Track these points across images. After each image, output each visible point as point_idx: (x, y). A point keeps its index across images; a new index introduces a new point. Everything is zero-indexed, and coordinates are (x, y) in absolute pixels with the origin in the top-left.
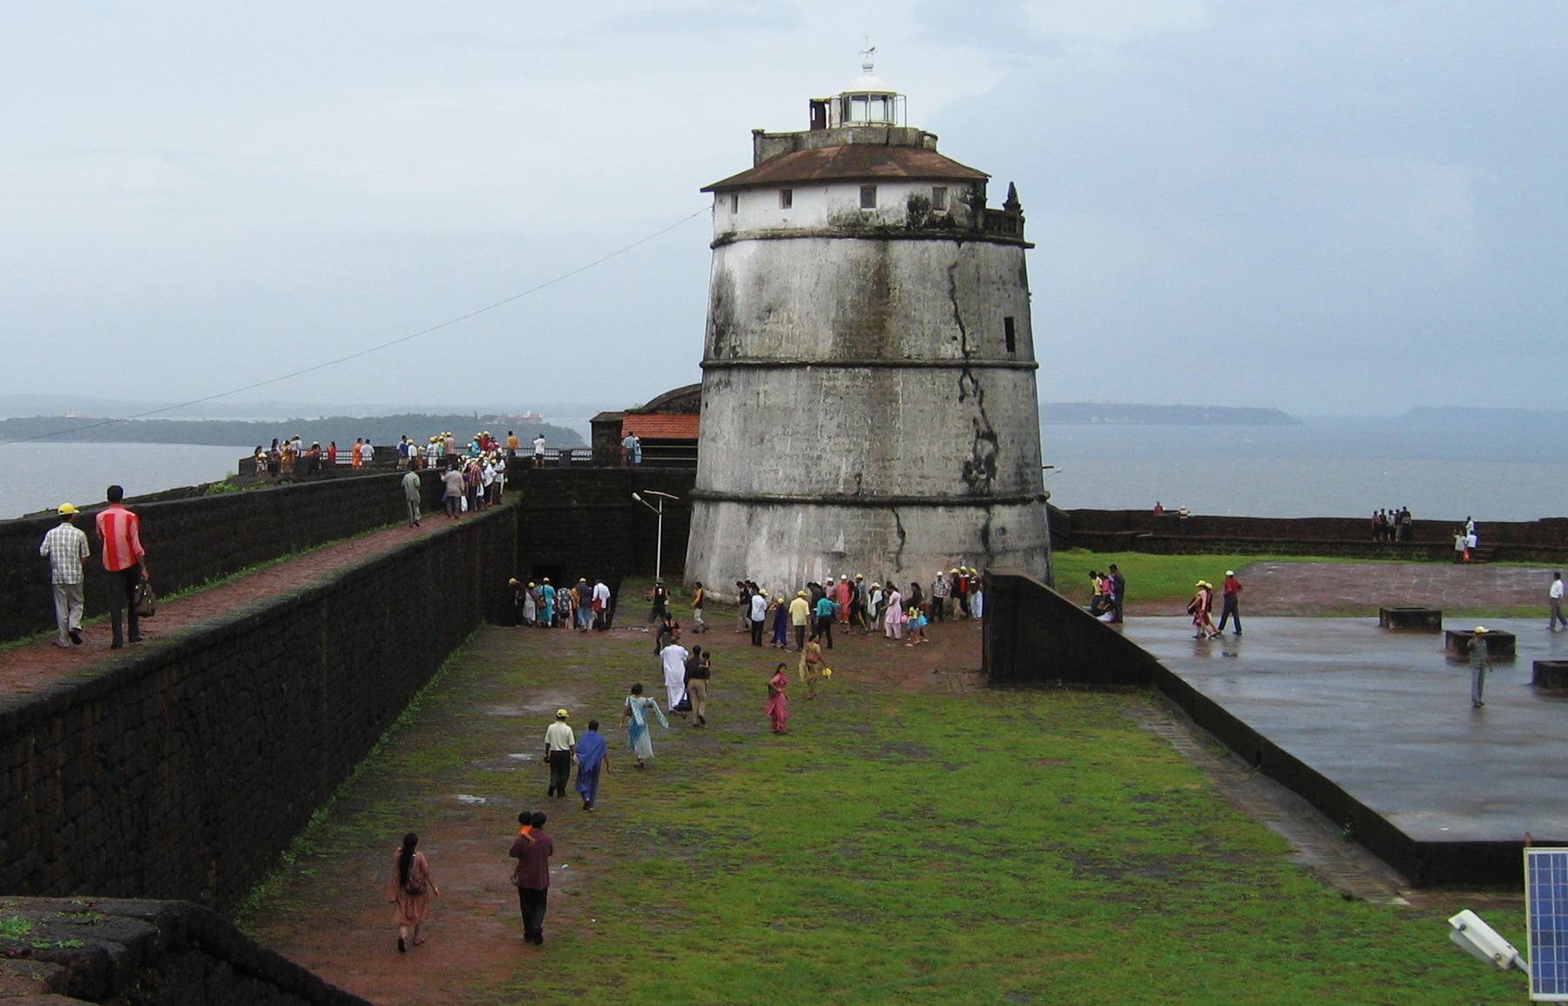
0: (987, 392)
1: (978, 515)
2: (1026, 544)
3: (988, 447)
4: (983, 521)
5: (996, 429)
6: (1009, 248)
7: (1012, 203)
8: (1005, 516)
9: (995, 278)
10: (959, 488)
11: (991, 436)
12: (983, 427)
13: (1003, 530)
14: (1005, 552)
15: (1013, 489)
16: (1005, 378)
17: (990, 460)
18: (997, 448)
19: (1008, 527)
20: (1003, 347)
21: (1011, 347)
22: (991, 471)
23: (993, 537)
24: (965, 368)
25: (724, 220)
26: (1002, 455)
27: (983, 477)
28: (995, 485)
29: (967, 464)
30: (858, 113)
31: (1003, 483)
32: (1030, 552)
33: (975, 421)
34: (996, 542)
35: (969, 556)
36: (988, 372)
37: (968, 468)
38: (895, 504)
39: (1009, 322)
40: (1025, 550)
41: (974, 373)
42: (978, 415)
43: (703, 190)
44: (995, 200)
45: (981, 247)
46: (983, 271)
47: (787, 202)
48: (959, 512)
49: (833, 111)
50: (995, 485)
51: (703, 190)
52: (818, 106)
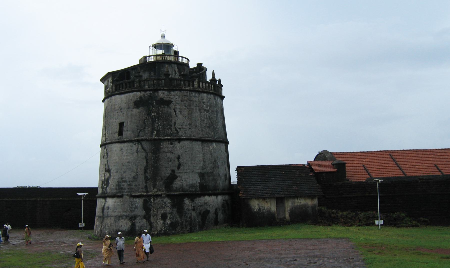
0: (109, 153)
2: (116, 214)
4: (103, 204)
5: (110, 168)
6: (127, 95)
8: (110, 202)
9: (117, 108)
11: (108, 171)
12: (107, 168)
13: (108, 208)
14: (108, 216)
15: (115, 191)
16: (116, 147)
17: (108, 179)
19: (110, 207)
20: (117, 135)
23: (105, 210)
26: (112, 177)
27: (105, 187)
29: (103, 181)
31: (111, 189)
32: (119, 217)
33: (105, 165)
36: (110, 146)
39: (121, 125)
40: (115, 217)
41: (107, 146)
42: (106, 162)
45: (113, 97)
46: (113, 107)
50: (108, 190)
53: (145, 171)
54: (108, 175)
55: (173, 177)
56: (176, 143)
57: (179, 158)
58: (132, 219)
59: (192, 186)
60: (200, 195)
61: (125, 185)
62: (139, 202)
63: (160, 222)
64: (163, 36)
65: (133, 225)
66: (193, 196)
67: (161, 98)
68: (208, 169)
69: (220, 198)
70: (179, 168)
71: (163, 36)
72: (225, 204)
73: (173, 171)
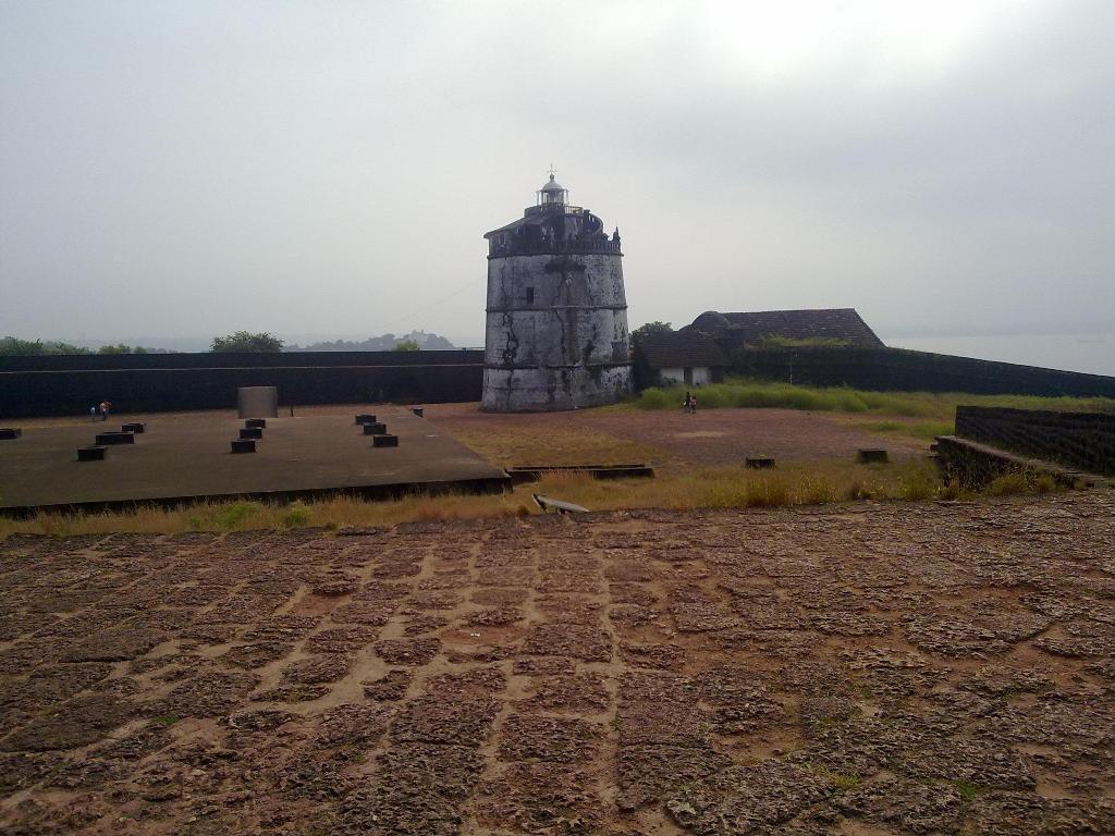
1: (506, 374)
2: (530, 386)
10: (502, 362)
13: (518, 380)
17: (515, 349)
18: (518, 345)
22: (515, 355)
28: (516, 360)
34: (513, 386)
35: (501, 389)
37: (505, 352)
42: (509, 330)
48: (500, 371)
50: (516, 360)
53: (562, 343)
54: (513, 344)
55: (589, 349)
56: (591, 312)
57: (594, 328)
58: (551, 391)
59: (606, 357)
60: (614, 366)
61: (540, 356)
62: (558, 374)
63: (579, 394)
64: (552, 177)
65: (552, 397)
66: (608, 367)
67: (553, 252)
68: (619, 339)
69: (628, 368)
70: (595, 338)
71: (552, 177)
72: (632, 371)
73: (590, 342)
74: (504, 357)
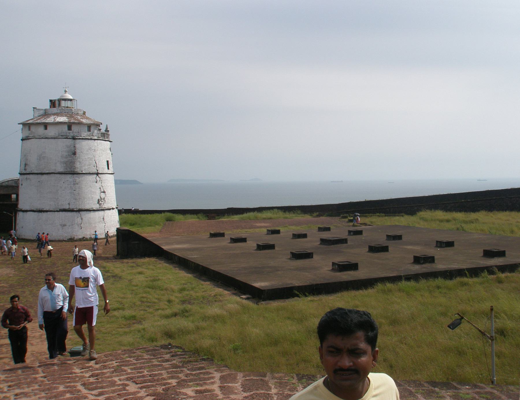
3: (103, 195)
7: (107, 130)
11: (104, 192)
21: (108, 169)
24: (97, 174)
25: (27, 133)
29: (98, 200)
30: (63, 103)
38: (80, 211)
41: (99, 175)
43: (19, 124)
44: (103, 128)
47: (46, 128)
48: (97, 213)
49: (57, 103)
51: (19, 124)
52: (51, 101)
74: (98, 203)
